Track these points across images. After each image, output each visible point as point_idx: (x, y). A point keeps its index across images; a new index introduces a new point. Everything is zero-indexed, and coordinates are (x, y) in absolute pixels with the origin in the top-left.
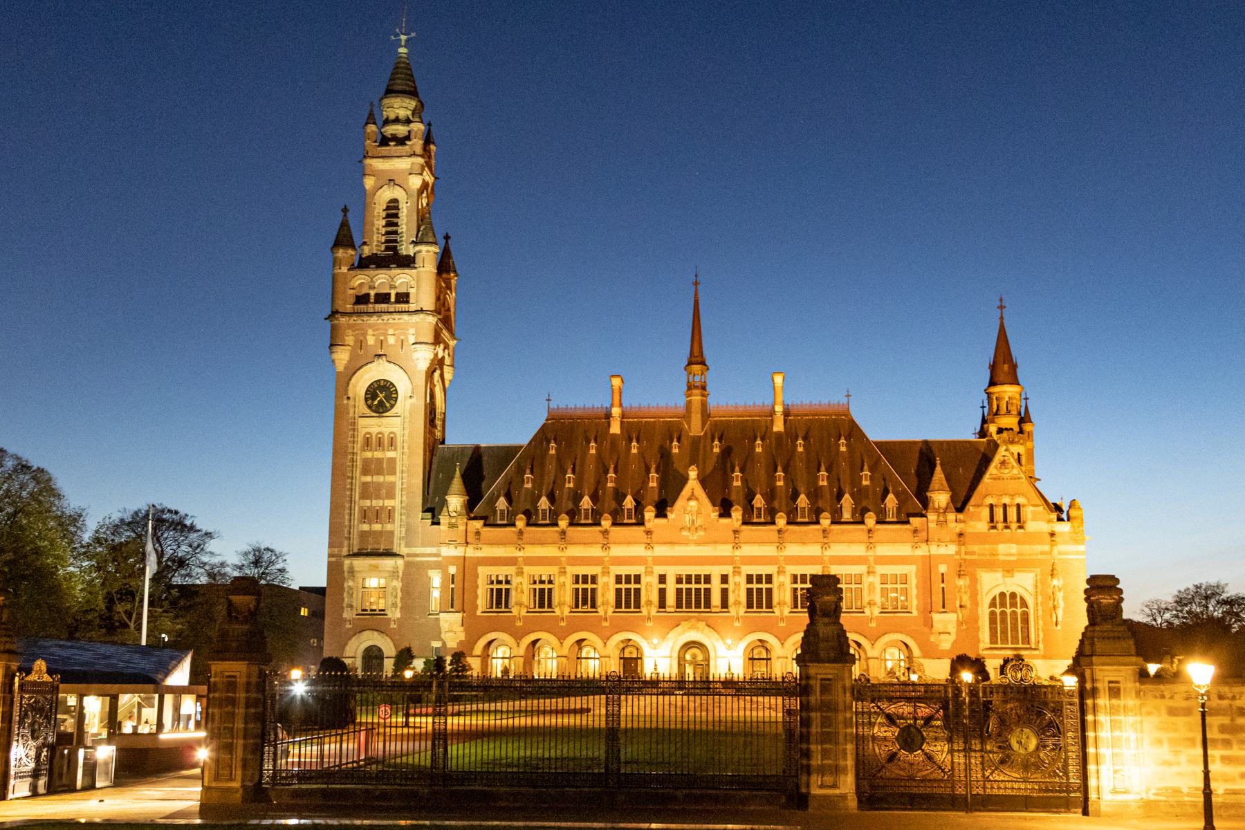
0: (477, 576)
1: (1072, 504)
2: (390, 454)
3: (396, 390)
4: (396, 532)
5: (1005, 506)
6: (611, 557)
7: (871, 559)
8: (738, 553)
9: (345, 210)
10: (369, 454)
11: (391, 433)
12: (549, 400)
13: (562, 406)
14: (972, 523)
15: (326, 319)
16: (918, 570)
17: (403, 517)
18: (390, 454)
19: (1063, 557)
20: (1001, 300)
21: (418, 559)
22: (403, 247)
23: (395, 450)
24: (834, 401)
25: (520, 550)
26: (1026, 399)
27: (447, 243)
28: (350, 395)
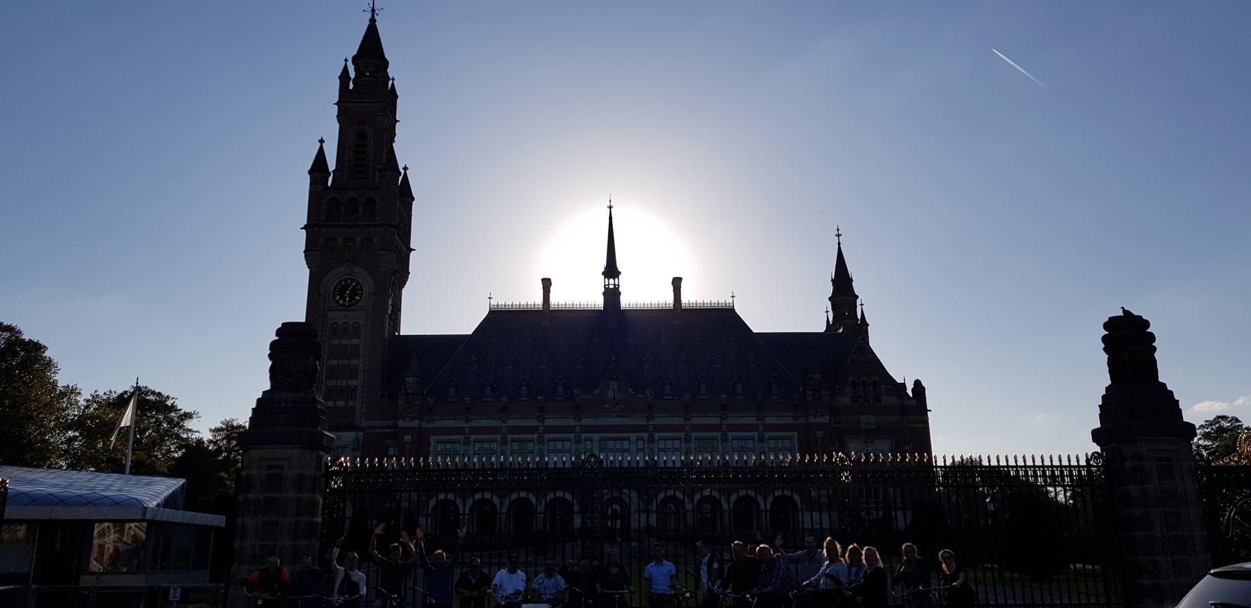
0: (429, 444)
1: (918, 384)
2: (355, 341)
3: (361, 288)
4: (357, 409)
5: (864, 382)
6: (545, 427)
7: (761, 427)
8: (651, 423)
9: (322, 141)
10: (336, 342)
11: (355, 323)
12: (490, 298)
13: (501, 303)
14: (839, 398)
15: (301, 229)
16: (798, 434)
17: (364, 394)
18: (355, 341)
19: (911, 425)
20: (838, 230)
21: (377, 430)
22: (370, 172)
23: (359, 338)
24: (722, 301)
25: (467, 422)
26: (862, 305)
27: (405, 173)
28: (321, 292)
